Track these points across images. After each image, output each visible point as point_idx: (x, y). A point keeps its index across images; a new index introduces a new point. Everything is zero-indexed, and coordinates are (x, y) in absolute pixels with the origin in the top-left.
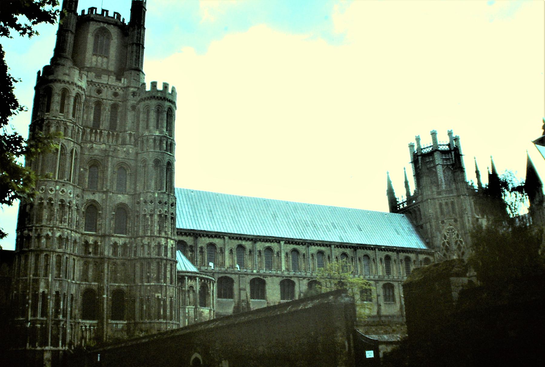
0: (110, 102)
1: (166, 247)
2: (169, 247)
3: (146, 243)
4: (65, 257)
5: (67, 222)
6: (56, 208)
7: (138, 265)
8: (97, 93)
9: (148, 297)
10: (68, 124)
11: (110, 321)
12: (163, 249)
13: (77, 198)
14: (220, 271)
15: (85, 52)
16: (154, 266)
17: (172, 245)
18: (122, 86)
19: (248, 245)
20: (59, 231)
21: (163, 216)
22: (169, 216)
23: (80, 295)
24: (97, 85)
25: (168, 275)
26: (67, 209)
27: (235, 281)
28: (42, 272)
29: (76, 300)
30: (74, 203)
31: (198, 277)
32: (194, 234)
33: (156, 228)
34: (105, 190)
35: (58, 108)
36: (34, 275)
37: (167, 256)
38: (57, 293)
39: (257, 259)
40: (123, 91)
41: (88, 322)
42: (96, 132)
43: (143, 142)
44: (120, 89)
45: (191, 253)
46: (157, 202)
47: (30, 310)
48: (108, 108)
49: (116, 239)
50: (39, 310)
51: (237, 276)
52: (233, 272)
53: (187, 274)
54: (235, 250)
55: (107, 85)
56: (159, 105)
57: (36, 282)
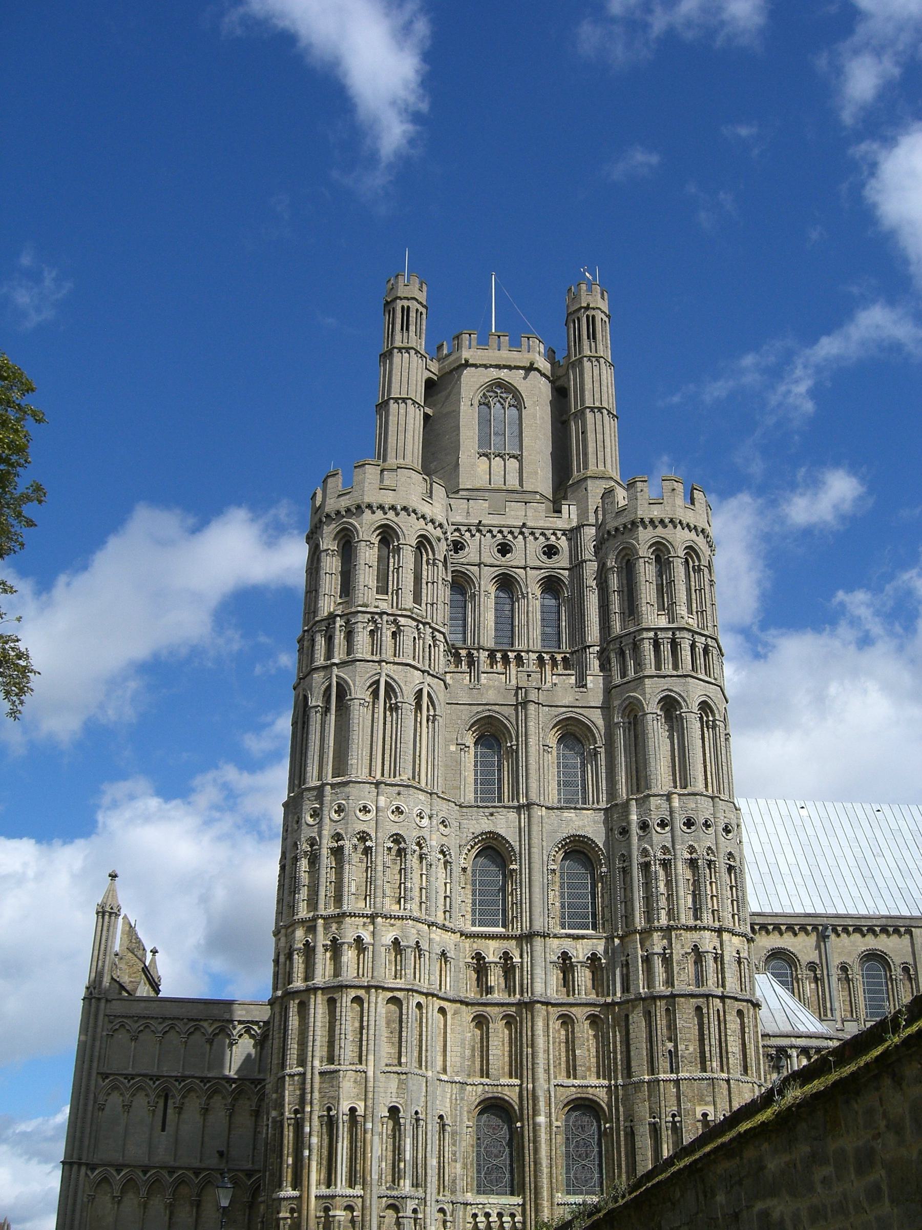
0: (538, 572)
1: (719, 959)
3: (658, 949)
4: (413, 1003)
5: (417, 900)
6: (382, 858)
8: (499, 551)
9: (674, 1116)
10: (402, 621)
12: (710, 964)
13: (441, 827)
18: (568, 527)
20: (392, 925)
23: (465, 1119)
24: (495, 531)
25: (734, 1047)
26: (413, 861)
28: (348, 1051)
29: (454, 1133)
32: (815, 928)
35: (373, 583)
37: (723, 986)
38: (394, 1111)
44: (559, 533)
48: (535, 589)
49: (568, 945)
53: (794, 1041)
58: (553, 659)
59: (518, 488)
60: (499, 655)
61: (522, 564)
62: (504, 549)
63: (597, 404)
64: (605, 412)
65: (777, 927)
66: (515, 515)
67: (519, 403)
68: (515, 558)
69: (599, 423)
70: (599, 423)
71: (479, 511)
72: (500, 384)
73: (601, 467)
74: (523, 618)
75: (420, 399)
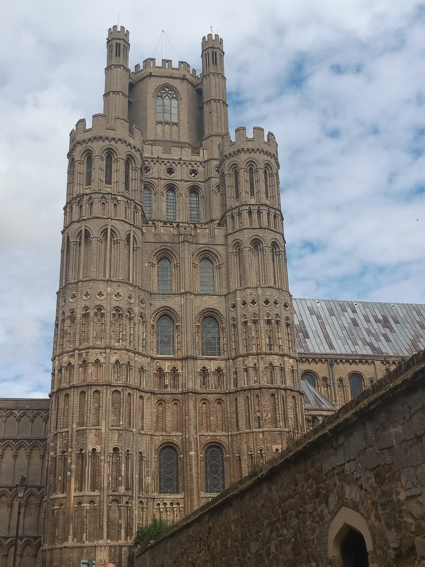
0: (188, 183)
1: (282, 369)
2: (287, 370)
7: (241, 400)
8: (168, 172)
9: (261, 450)
10: (119, 198)
13: (141, 304)
17: (292, 367)
20: (115, 353)
23: (153, 454)
24: (166, 161)
25: (291, 414)
30: (137, 312)
33: (265, 341)
36: (79, 424)
38: (116, 449)
40: (204, 167)
43: (233, 217)
44: (198, 164)
45: (325, 389)
47: (73, 480)
50: (88, 481)
53: (320, 412)
55: (181, 162)
57: (82, 433)
59: (177, 140)
62: (170, 171)
63: (218, 98)
64: (221, 101)
65: (307, 360)
75: (127, 93)
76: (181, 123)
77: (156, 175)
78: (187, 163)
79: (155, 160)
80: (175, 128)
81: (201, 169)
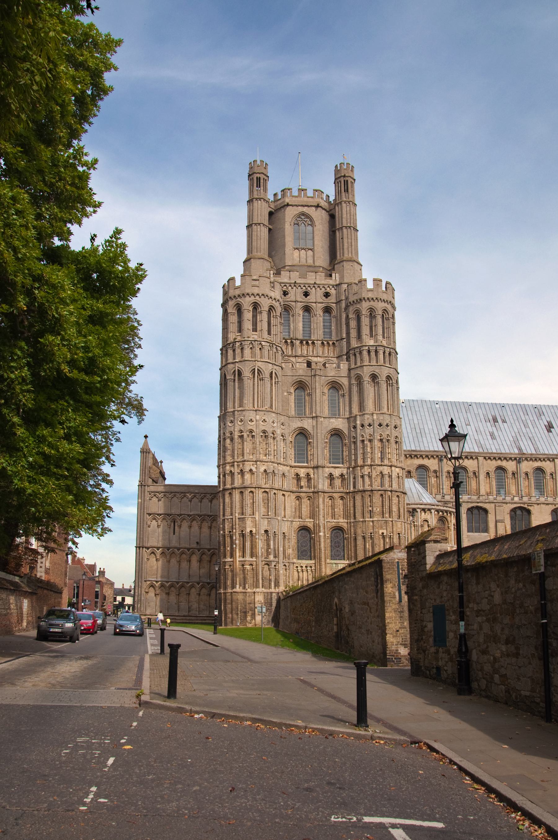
0: (321, 305)
5: (273, 455)
8: (304, 295)
9: (371, 533)
11: (328, 561)
14: (470, 500)
15: (284, 246)
16: (377, 499)
18: (335, 284)
19: (510, 466)
21: (384, 440)
22: (393, 440)
24: (302, 286)
27: (490, 511)
28: (248, 510)
29: (289, 539)
30: (279, 433)
31: (434, 509)
32: (437, 456)
34: (314, 415)
38: (266, 531)
39: (524, 483)
40: (336, 289)
41: (304, 561)
42: (307, 343)
44: (331, 287)
46: (376, 425)
49: (332, 470)
51: (493, 505)
52: (487, 501)
54: (493, 473)
55: (315, 285)
56: (371, 308)
58: (328, 343)
59: (312, 264)
60: (304, 342)
61: (314, 301)
62: (306, 294)
65: (421, 456)
66: (311, 278)
67: (312, 224)
68: (311, 298)
69: (349, 234)
70: (349, 234)
71: (295, 277)
72: (303, 214)
73: (350, 255)
74: (315, 325)
76: (315, 248)
77: (293, 298)
78: (321, 286)
79: (293, 285)
80: (310, 253)
81: (333, 291)
